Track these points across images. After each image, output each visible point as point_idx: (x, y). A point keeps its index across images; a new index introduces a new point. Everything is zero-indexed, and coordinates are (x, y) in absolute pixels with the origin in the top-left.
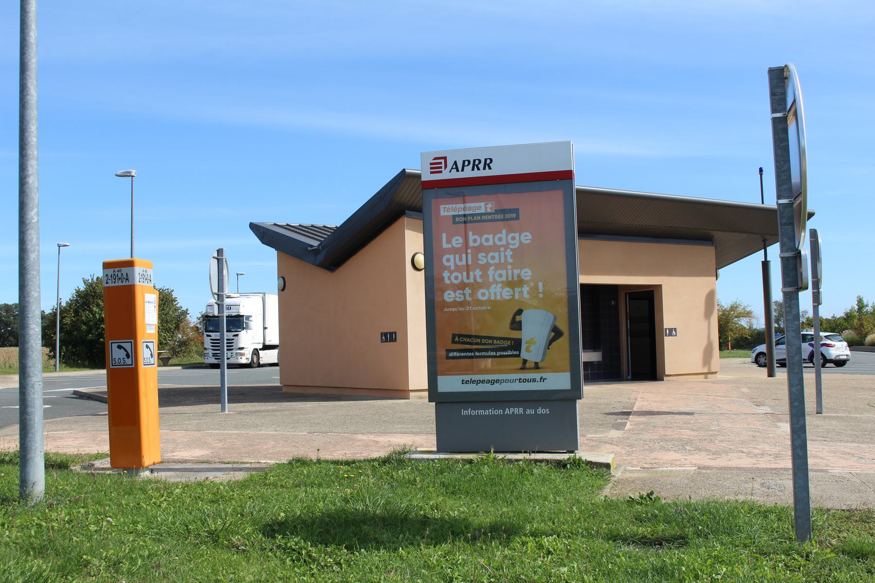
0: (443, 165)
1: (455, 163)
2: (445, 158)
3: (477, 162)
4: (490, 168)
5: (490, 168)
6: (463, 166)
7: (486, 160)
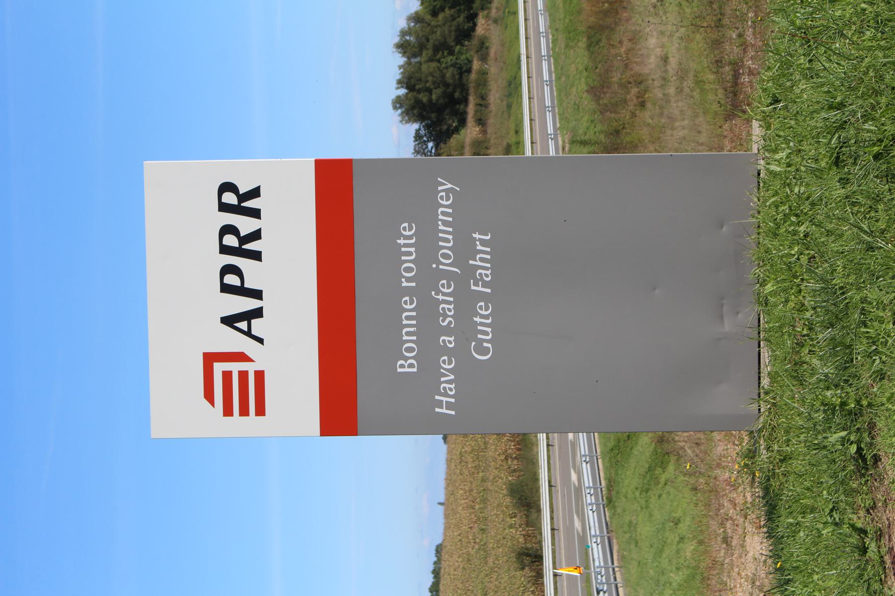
0: (235, 367)
1: (229, 321)
2: (210, 359)
3: (231, 241)
4: (255, 193)
5: (255, 193)
6: (241, 291)
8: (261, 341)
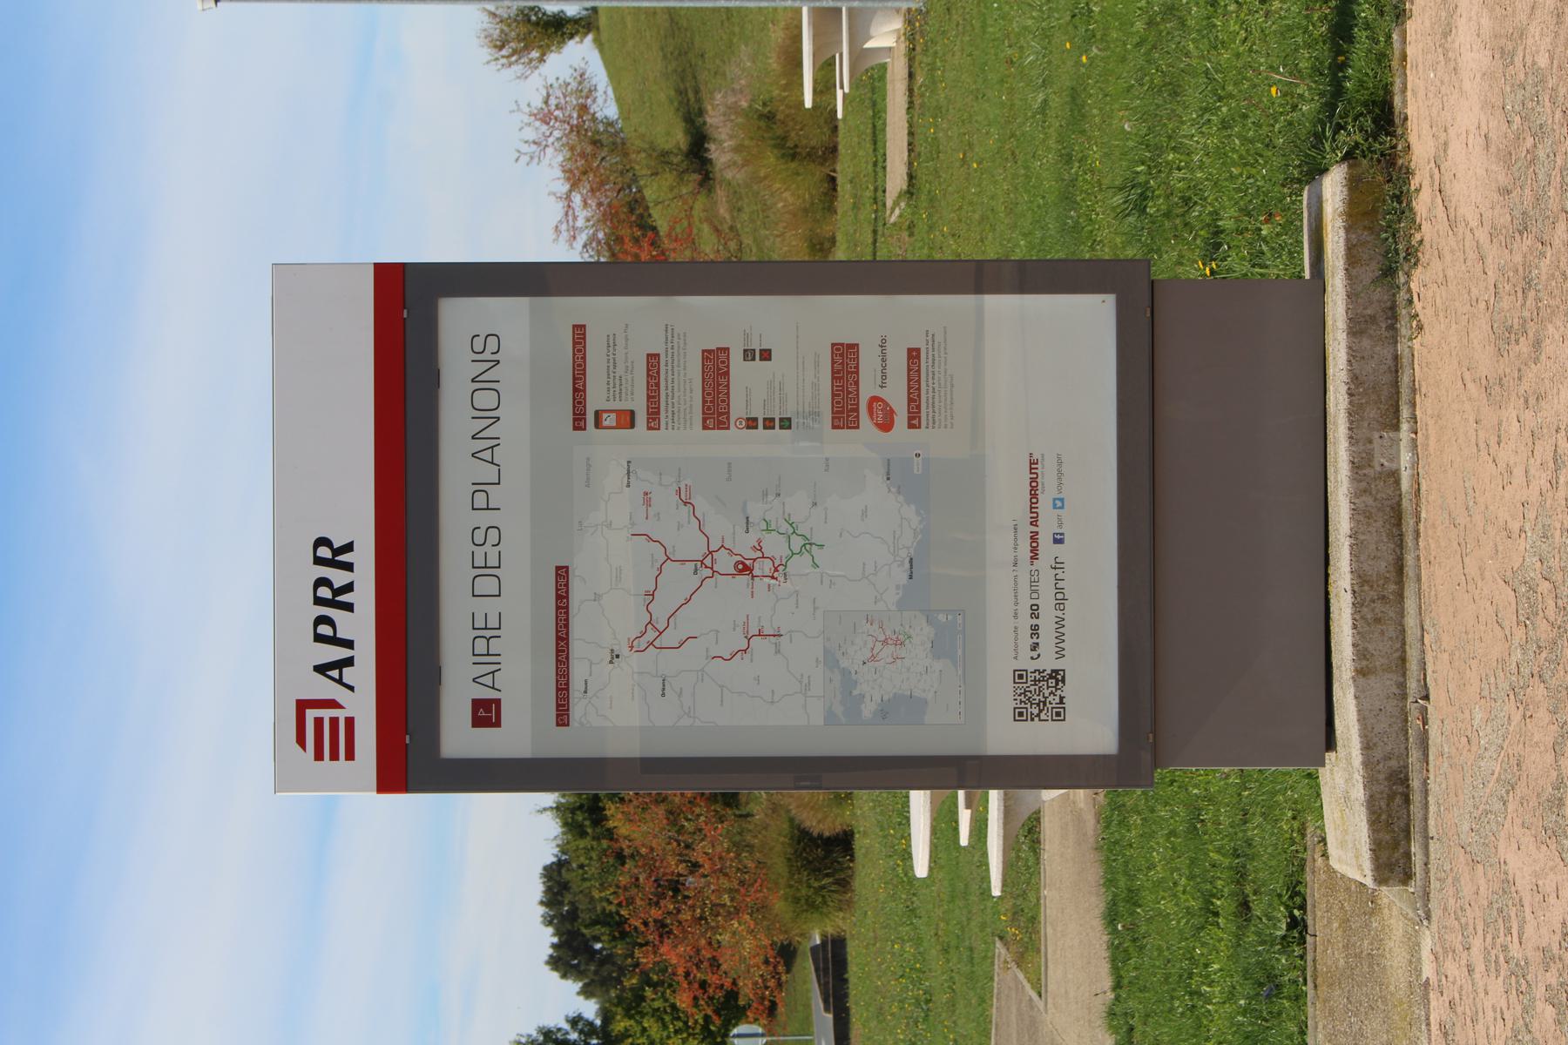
0: (326, 714)
1: (321, 669)
2: (302, 706)
3: (325, 592)
4: (349, 547)
5: (349, 547)
7: (318, 561)
8: (351, 688)
